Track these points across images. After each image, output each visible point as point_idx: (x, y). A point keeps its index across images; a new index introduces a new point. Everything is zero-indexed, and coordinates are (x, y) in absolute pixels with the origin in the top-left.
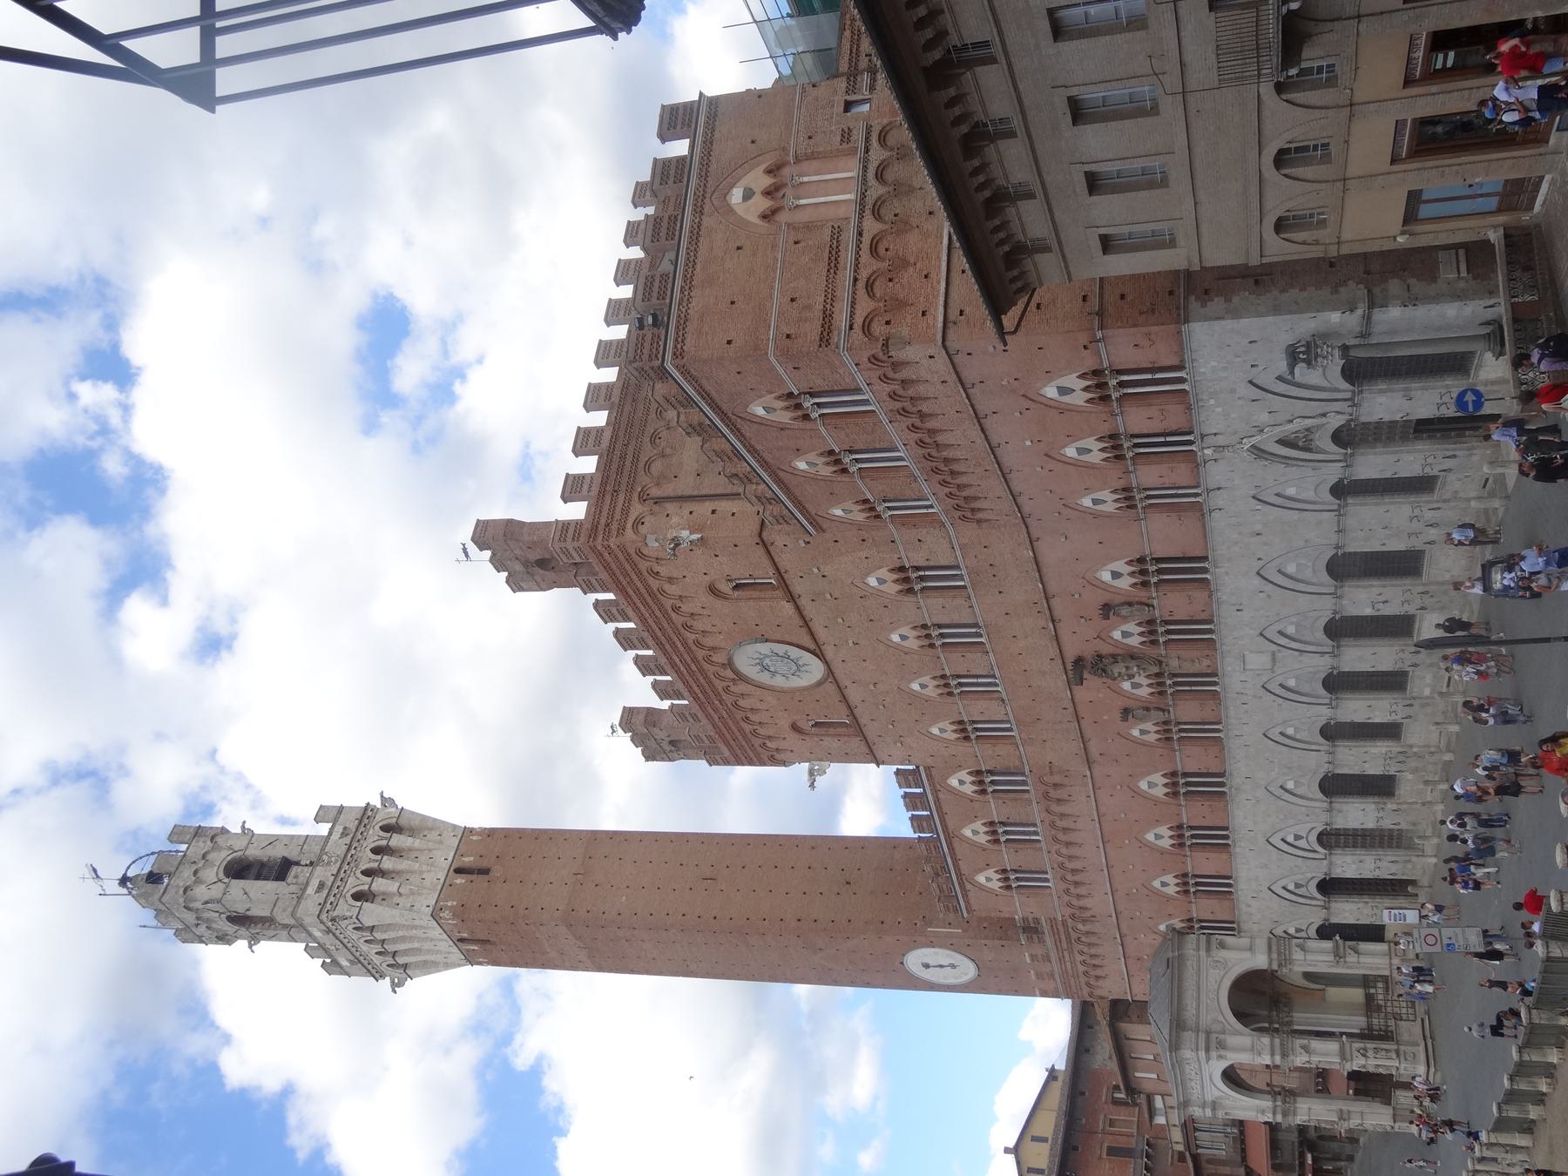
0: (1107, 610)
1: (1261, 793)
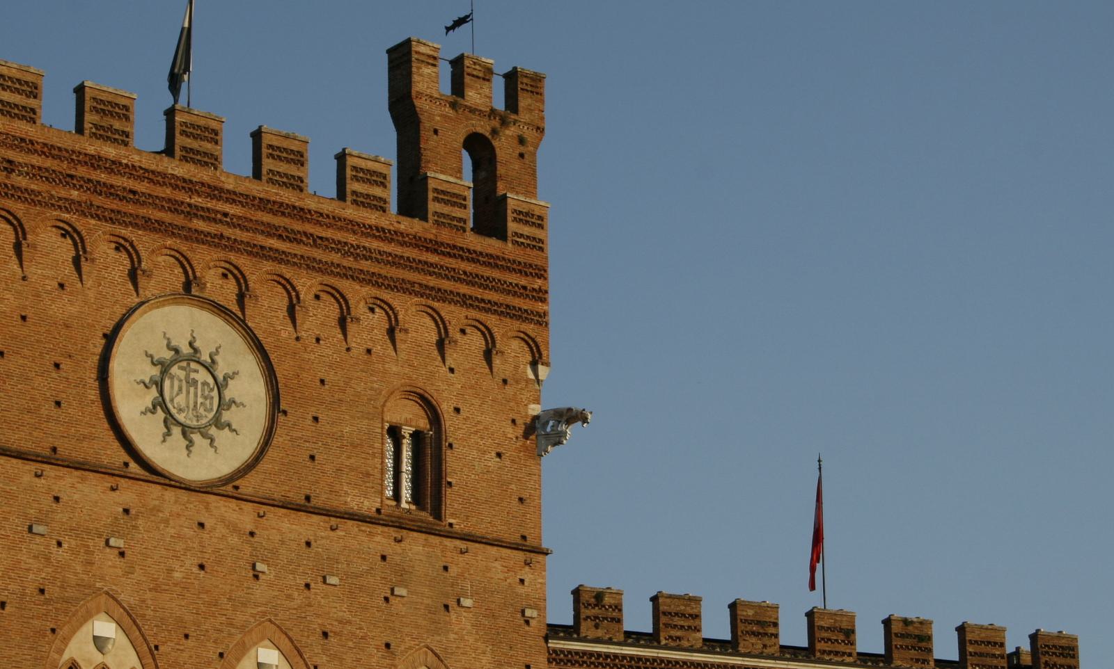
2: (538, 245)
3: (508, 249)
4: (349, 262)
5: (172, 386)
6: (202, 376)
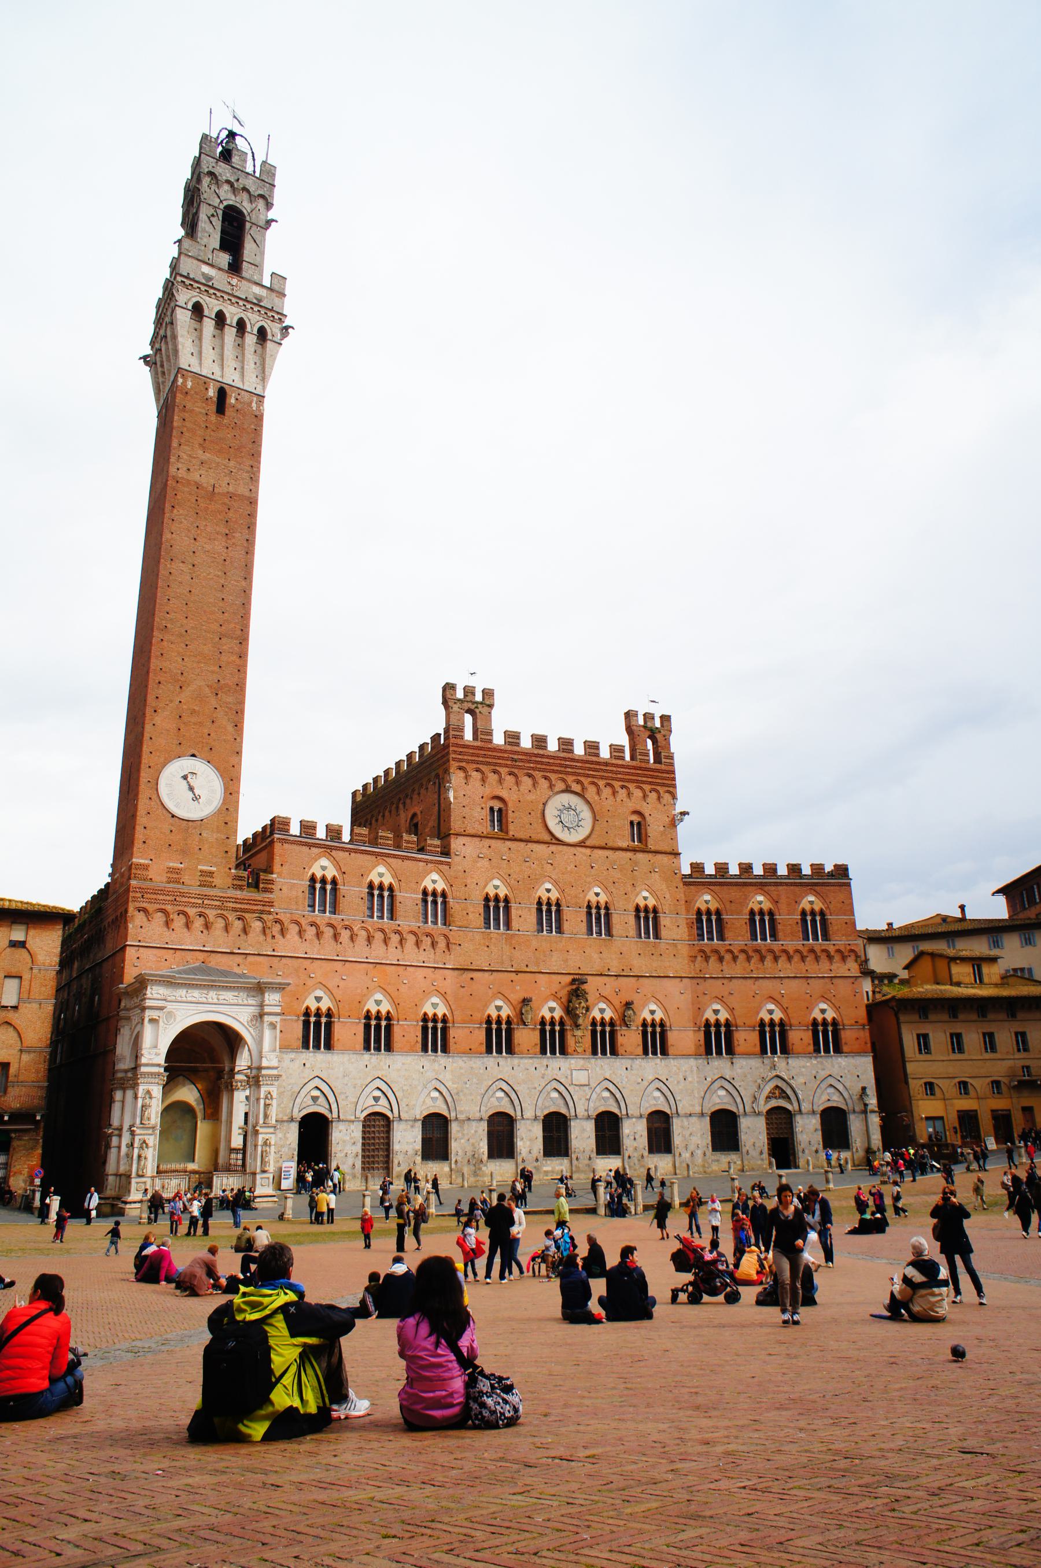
0: (628, 1005)
1: (431, 1075)
2: (672, 765)
3: (663, 767)
4: (614, 776)
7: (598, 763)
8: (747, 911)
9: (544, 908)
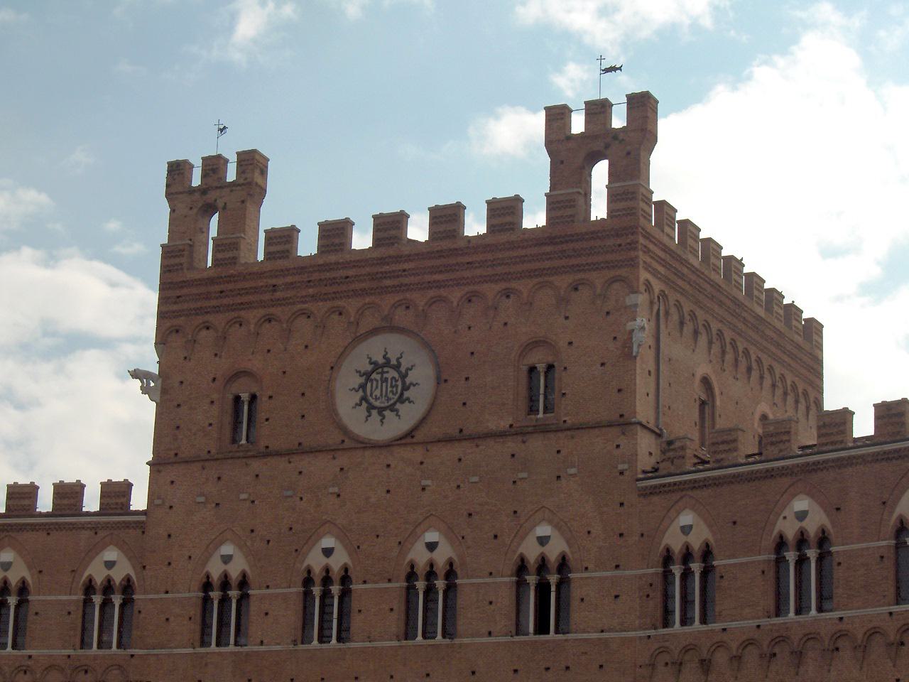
5: (372, 387)
6: (392, 374)
7: (455, 252)
8: (769, 541)
9: (317, 590)
